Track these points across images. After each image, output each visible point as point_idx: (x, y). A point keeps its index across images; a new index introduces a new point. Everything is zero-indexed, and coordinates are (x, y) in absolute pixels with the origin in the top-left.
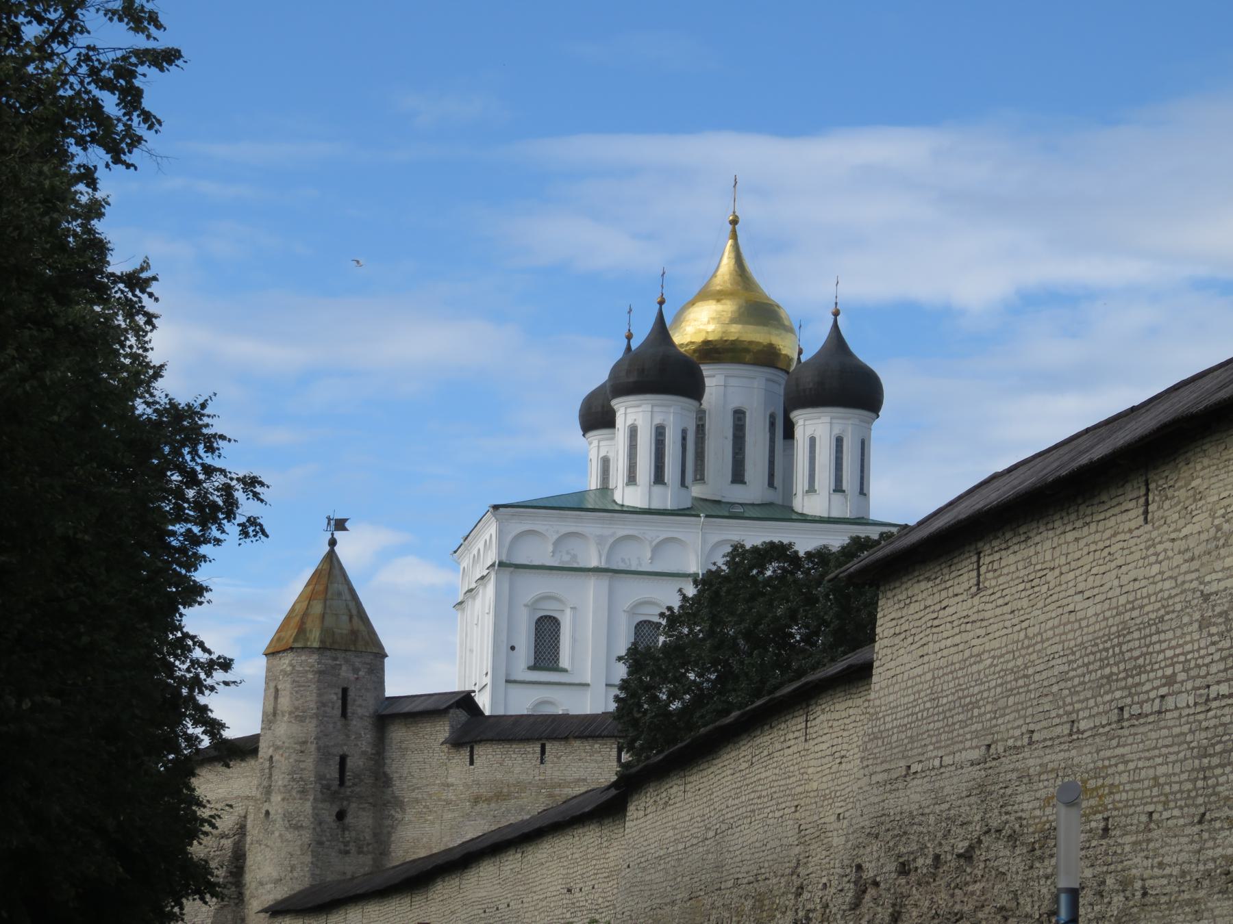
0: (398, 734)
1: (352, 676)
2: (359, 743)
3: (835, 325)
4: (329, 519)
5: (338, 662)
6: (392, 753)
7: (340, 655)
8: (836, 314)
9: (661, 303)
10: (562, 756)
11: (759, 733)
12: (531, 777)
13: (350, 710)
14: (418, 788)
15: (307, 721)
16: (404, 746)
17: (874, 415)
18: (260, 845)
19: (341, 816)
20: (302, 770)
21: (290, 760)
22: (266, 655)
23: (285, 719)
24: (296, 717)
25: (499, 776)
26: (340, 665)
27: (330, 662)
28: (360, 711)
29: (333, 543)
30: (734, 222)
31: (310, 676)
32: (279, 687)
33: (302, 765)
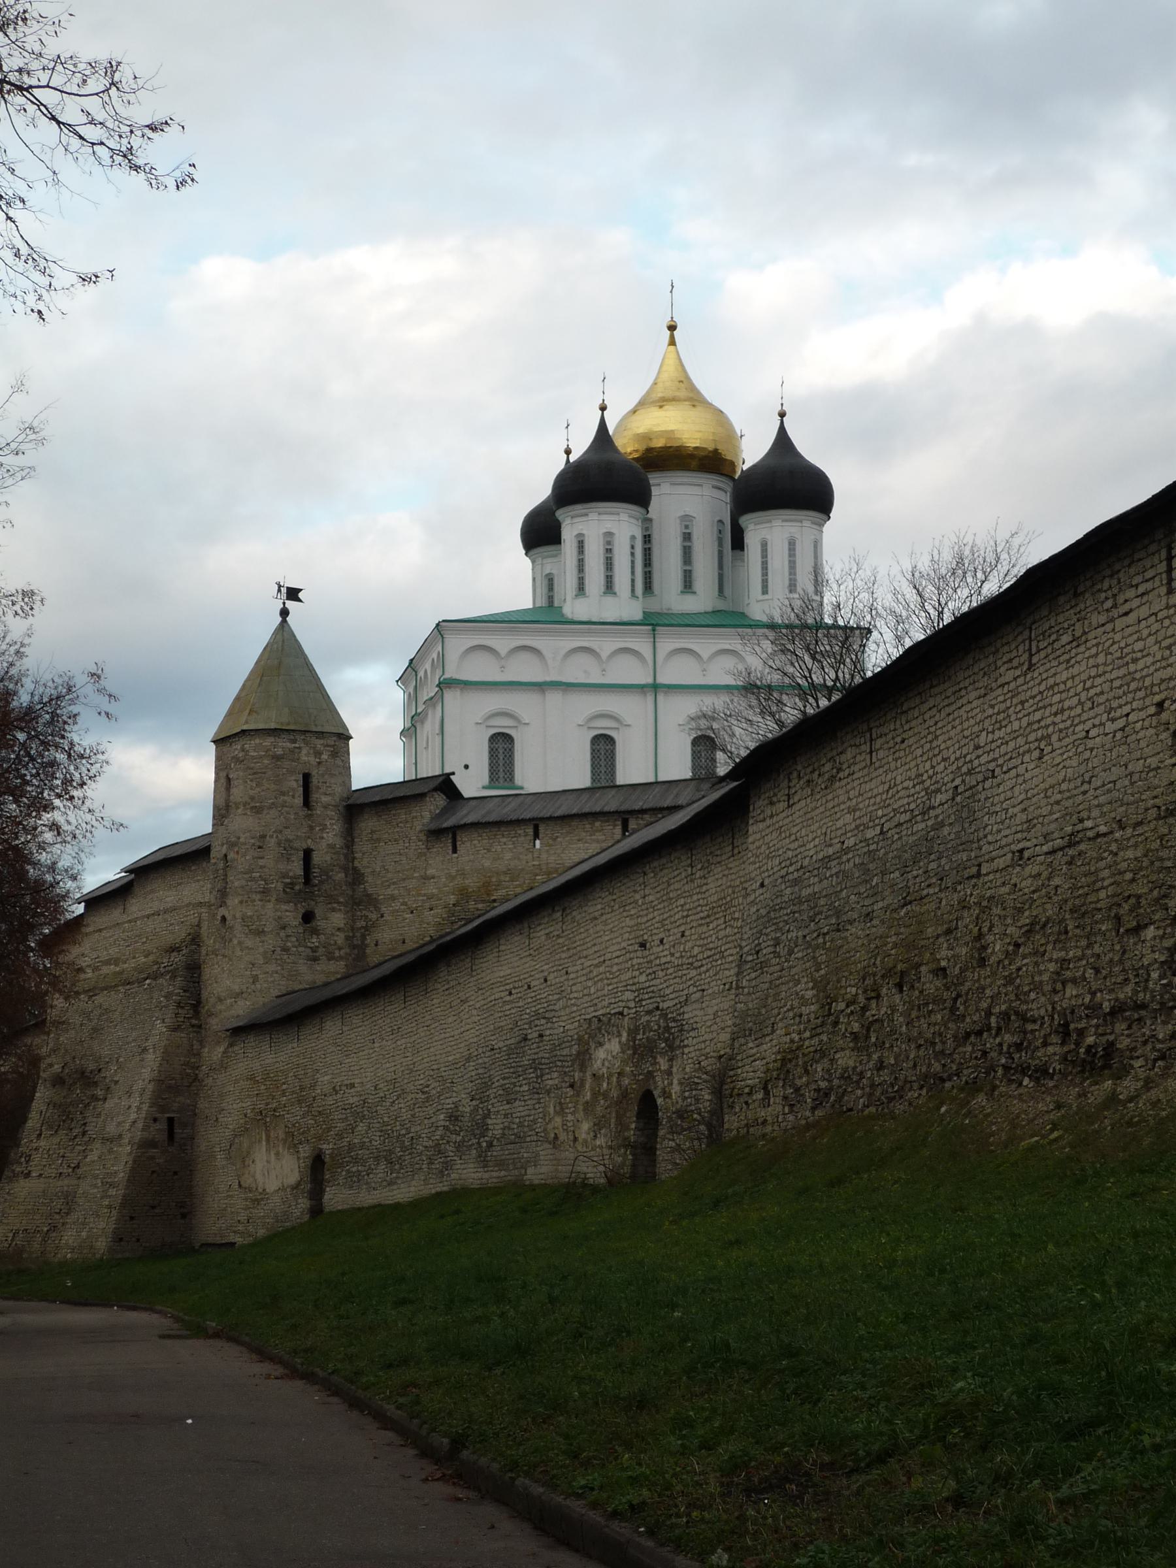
0: (368, 824)
1: (313, 760)
2: (325, 835)
3: (782, 430)
4: (280, 586)
5: (297, 745)
6: (362, 846)
7: (300, 737)
8: (782, 415)
9: (603, 408)
10: (557, 837)
11: (1045, 612)
12: (524, 862)
13: (314, 796)
14: (394, 883)
15: (265, 812)
16: (375, 837)
17: (824, 517)
18: (217, 955)
19: (308, 917)
20: (261, 867)
21: (247, 858)
22: (214, 742)
23: (240, 811)
24: (252, 808)
25: (487, 864)
26: (299, 748)
27: (288, 745)
28: (325, 799)
29: (284, 613)
30: (672, 328)
31: (266, 762)
32: (231, 776)
33: (261, 862)
